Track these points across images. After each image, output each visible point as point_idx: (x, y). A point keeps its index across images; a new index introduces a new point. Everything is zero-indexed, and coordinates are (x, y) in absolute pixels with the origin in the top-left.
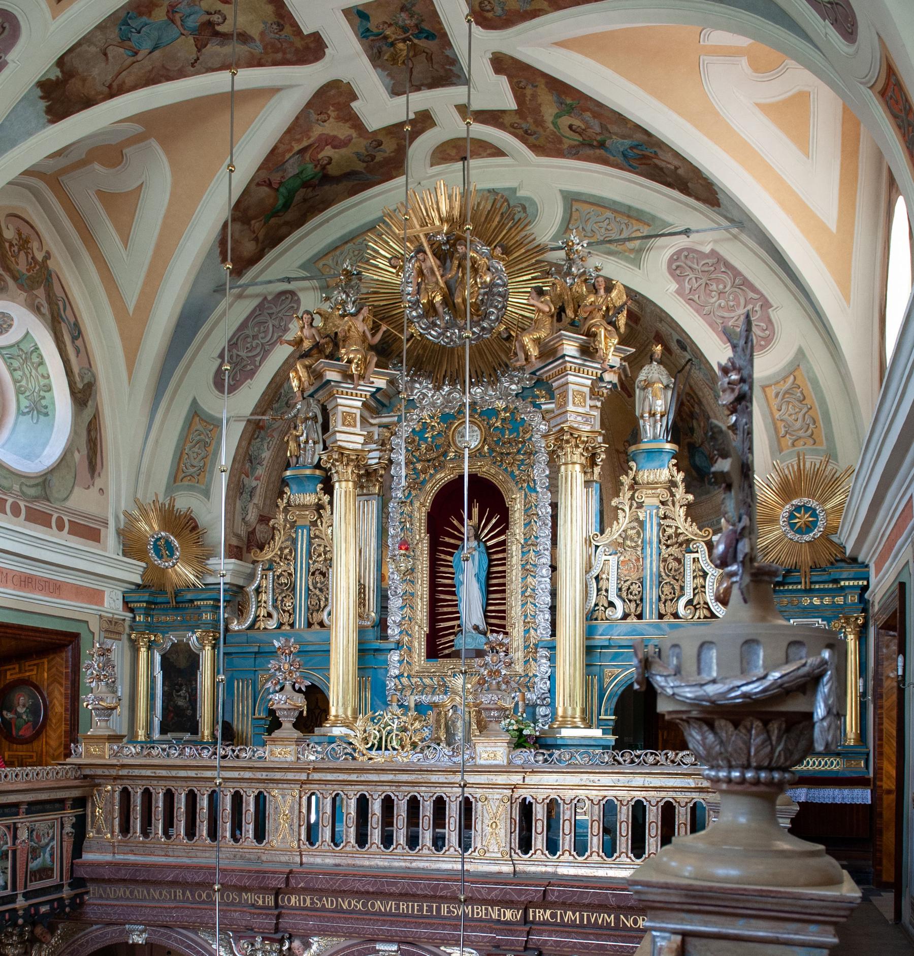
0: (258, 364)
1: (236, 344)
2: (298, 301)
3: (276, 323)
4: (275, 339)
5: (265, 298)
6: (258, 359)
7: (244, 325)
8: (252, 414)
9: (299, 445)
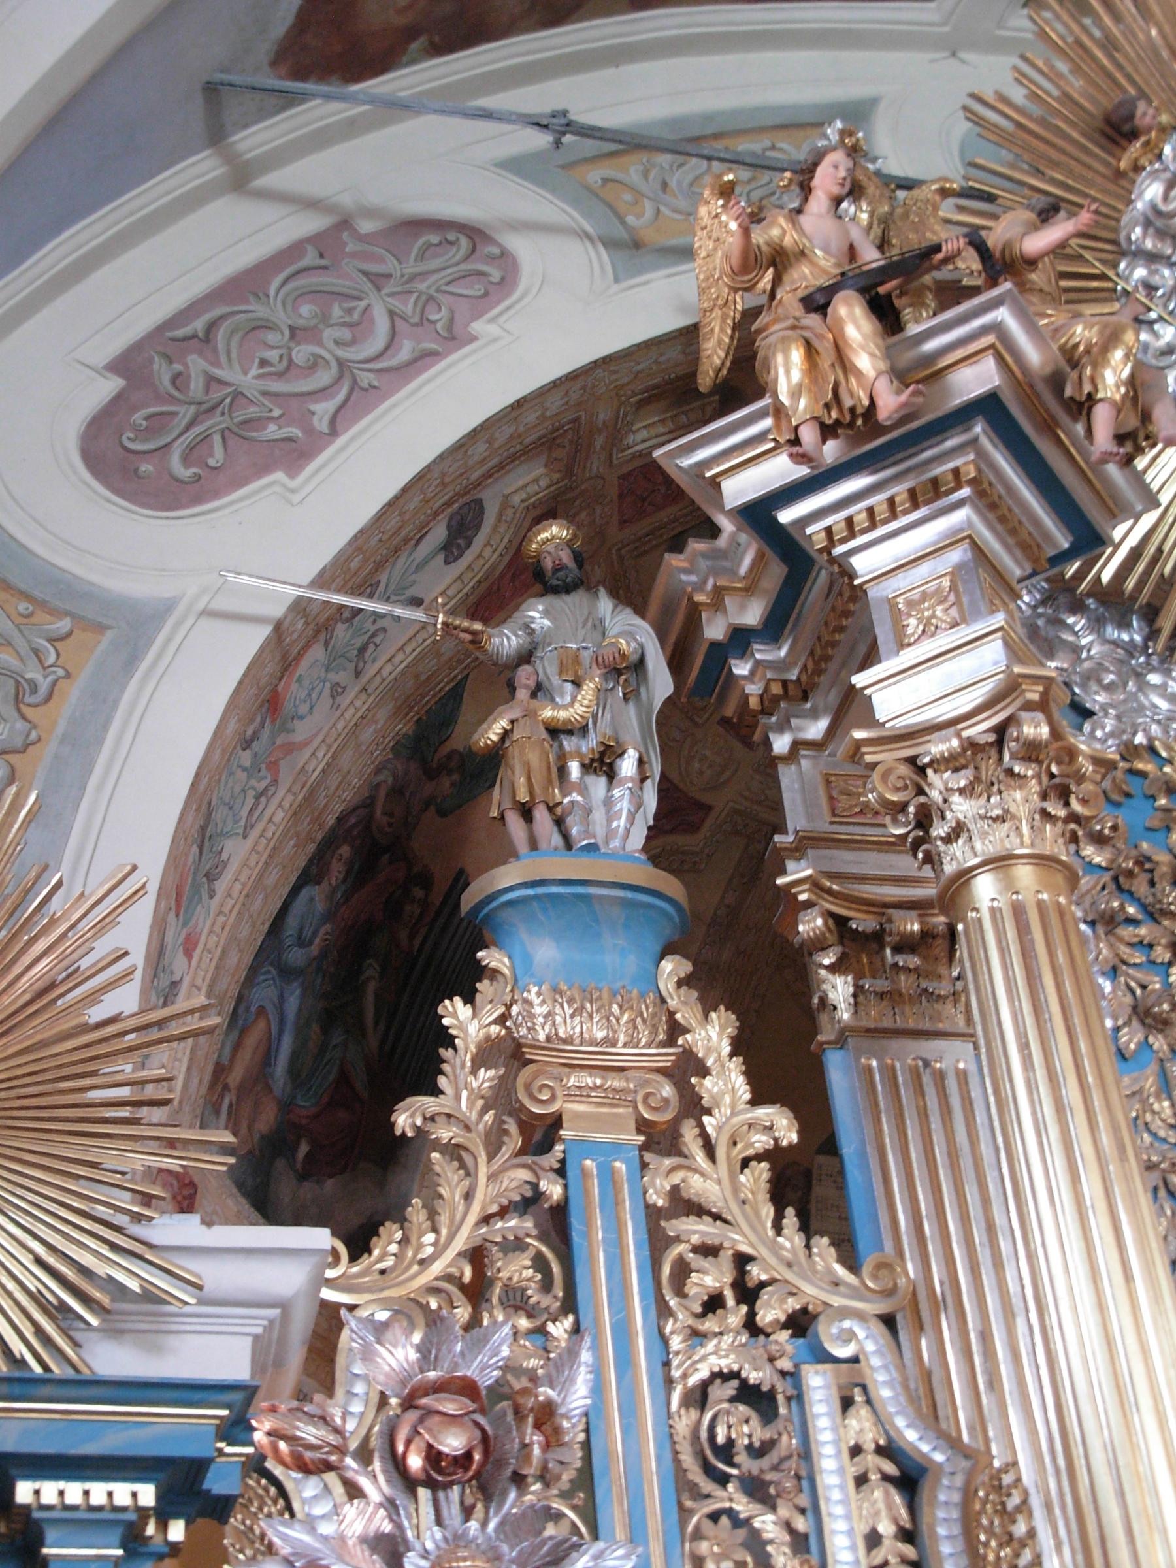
0: (321, 424)
1: (208, 336)
2: (506, 260)
3: (408, 307)
4: (405, 352)
5: (345, 224)
6: (323, 409)
7: (245, 285)
8: (322, 581)
9: (563, 771)
